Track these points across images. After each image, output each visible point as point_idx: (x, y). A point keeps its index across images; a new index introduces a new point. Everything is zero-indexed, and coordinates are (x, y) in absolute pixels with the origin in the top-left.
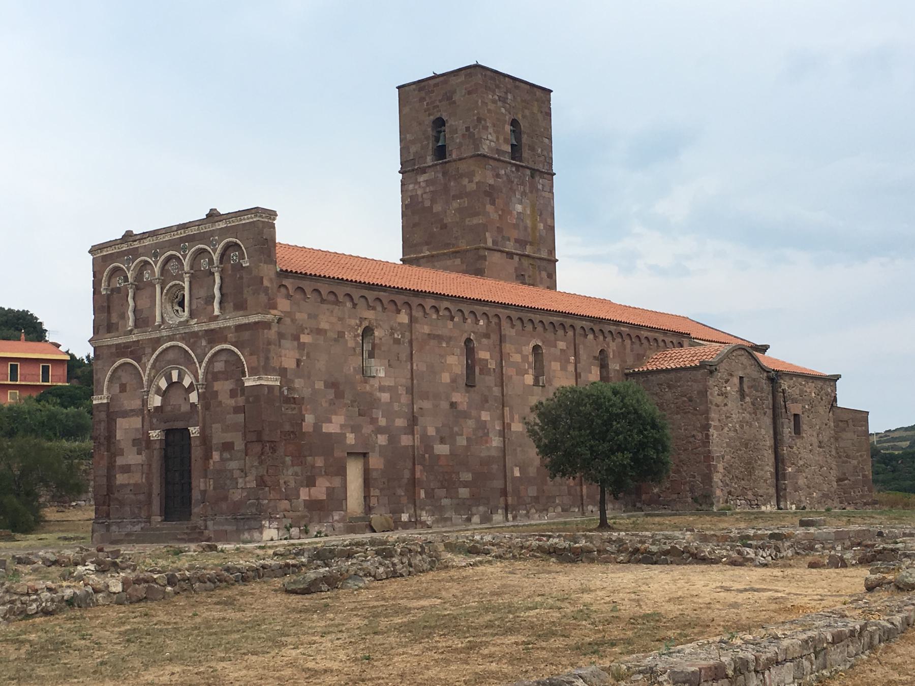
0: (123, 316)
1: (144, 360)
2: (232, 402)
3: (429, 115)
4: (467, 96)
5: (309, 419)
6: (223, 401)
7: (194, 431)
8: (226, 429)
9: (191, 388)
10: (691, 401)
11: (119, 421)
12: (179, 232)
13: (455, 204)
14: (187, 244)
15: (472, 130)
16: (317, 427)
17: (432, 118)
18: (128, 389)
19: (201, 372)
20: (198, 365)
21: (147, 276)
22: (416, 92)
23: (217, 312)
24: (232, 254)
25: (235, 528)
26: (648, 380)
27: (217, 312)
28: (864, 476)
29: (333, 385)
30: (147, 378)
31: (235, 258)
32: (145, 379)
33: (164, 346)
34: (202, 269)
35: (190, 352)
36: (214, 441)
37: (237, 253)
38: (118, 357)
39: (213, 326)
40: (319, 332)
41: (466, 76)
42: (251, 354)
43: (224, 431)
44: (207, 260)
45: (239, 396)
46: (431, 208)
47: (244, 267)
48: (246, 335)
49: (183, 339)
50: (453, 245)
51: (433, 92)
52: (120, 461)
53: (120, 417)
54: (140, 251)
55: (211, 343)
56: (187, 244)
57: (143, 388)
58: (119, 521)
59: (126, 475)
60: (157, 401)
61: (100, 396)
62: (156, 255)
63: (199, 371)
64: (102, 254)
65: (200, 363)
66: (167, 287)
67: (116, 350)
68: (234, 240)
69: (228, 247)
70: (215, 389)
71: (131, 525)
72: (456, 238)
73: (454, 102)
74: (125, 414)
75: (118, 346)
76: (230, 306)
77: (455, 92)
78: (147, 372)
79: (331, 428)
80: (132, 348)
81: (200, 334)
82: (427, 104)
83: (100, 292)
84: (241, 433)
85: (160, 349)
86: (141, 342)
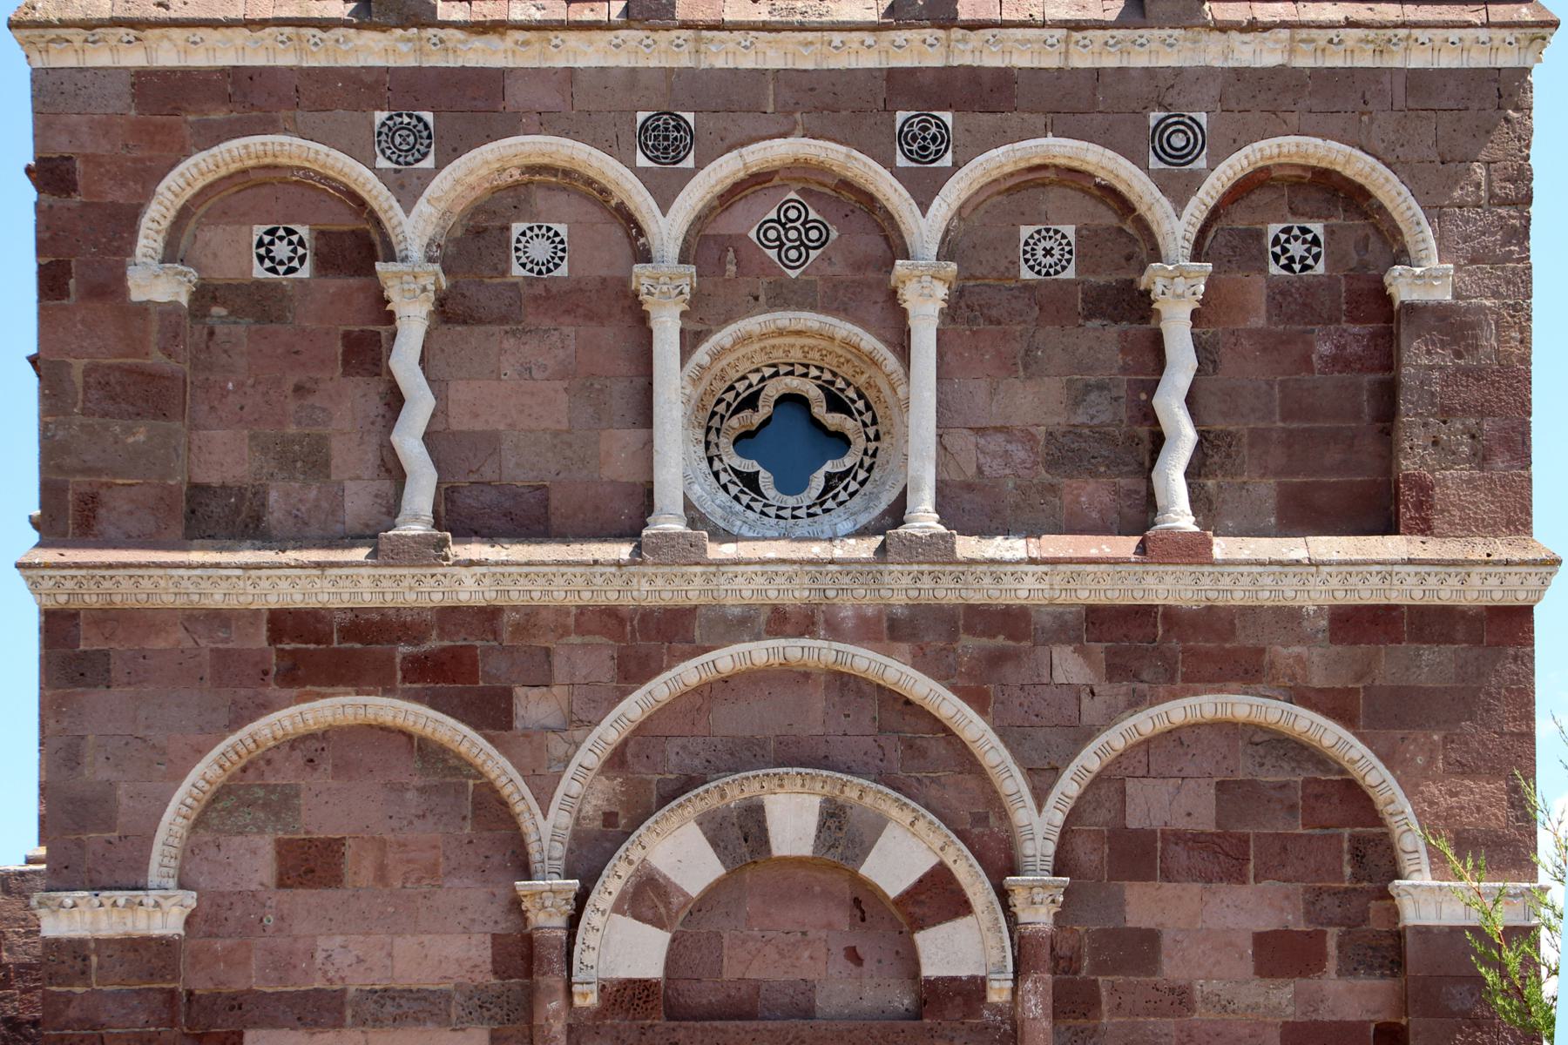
14: (947, 117)
31: (1296, 249)
44: (1070, 231)
54: (517, 97)
56: (947, 117)
66: (723, 337)
83: (110, 287)
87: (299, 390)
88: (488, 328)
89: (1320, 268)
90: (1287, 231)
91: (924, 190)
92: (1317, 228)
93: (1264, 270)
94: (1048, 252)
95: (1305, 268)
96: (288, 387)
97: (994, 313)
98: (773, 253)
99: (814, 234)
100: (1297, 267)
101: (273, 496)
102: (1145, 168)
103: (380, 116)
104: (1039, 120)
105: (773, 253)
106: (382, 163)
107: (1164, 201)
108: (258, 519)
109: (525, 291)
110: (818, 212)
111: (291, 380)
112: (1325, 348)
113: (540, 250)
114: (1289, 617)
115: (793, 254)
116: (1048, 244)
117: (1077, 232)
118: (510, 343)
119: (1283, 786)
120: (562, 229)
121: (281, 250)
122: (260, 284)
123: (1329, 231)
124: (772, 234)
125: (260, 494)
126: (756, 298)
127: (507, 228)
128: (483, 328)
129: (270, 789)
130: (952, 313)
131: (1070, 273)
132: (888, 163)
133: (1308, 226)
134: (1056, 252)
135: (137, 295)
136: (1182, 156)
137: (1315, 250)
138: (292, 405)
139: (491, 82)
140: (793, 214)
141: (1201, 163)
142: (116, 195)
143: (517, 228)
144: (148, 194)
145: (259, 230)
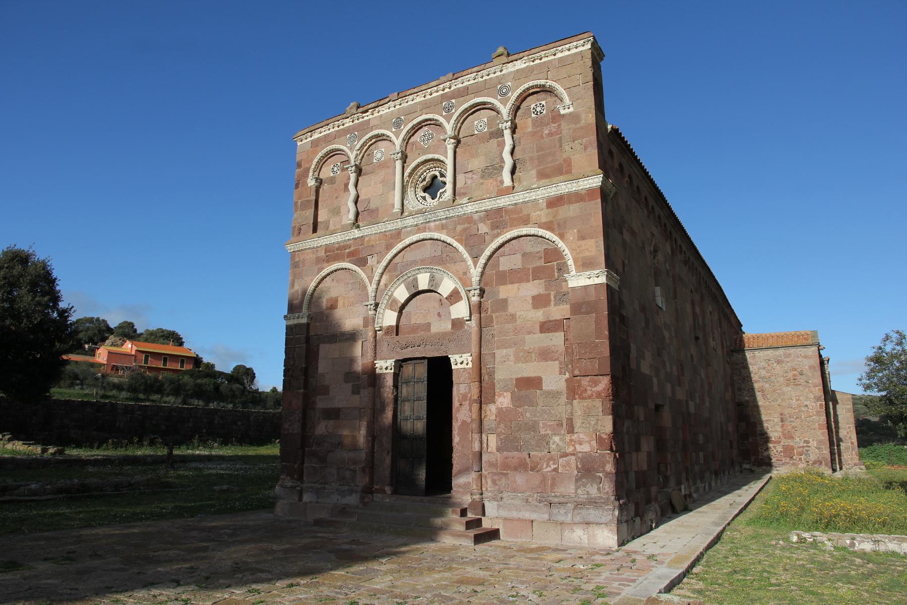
0: (336, 212)
1: (371, 262)
2: (539, 315)
5: (633, 347)
6: (518, 314)
8: (526, 356)
9: (454, 297)
10: (801, 374)
11: (325, 350)
12: (441, 86)
14: (453, 101)
16: (638, 364)
19: (475, 273)
20: (470, 262)
25: (546, 516)
26: (755, 356)
27: (507, 180)
28: (852, 443)
29: (643, 309)
30: (374, 286)
31: (539, 109)
32: (371, 289)
33: (407, 241)
34: (476, 132)
35: (456, 244)
36: (499, 376)
38: (328, 261)
39: (504, 201)
40: (633, 233)
42: (582, 237)
43: (517, 360)
44: (485, 120)
45: (552, 303)
47: (564, 115)
49: (443, 228)
52: (321, 403)
53: (324, 343)
55: (498, 227)
57: (368, 301)
58: (319, 486)
59: (332, 422)
60: (389, 318)
61: (297, 315)
62: (398, 124)
63: (472, 270)
64: (313, 138)
65: (475, 258)
67: (325, 253)
68: (542, 82)
69: (524, 97)
70: (502, 295)
71: (339, 495)
75: (328, 248)
76: (528, 175)
78: (376, 278)
79: (645, 368)
80: (352, 249)
81: (476, 217)
84: (557, 362)
85: (400, 246)
86: (366, 239)
87: (337, 197)
88: (369, 175)
90: (536, 105)
92: (543, 103)
93: (531, 116)
94: (481, 126)
95: (541, 113)
96: (335, 197)
97: (469, 144)
98: (422, 143)
99: (431, 136)
100: (539, 113)
101: (331, 222)
102: (497, 99)
103: (348, 136)
104: (473, 95)
105: (422, 143)
106: (348, 145)
107: (502, 105)
109: (376, 165)
110: (431, 131)
112: (546, 132)
113: (379, 155)
115: (426, 142)
116: (480, 124)
117: (488, 120)
118: (373, 177)
120: (383, 150)
121: (335, 169)
122: (332, 177)
123: (546, 102)
124: (422, 139)
125: (329, 221)
126: (419, 154)
127: (373, 153)
128: (368, 176)
131: (486, 130)
133: (541, 103)
134: (483, 126)
135: (309, 185)
136: (505, 94)
137: (543, 108)
140: (426, 133)
141: (510, 94)
142: (307, 166)
143: (375, 152)
144: (312, 163)
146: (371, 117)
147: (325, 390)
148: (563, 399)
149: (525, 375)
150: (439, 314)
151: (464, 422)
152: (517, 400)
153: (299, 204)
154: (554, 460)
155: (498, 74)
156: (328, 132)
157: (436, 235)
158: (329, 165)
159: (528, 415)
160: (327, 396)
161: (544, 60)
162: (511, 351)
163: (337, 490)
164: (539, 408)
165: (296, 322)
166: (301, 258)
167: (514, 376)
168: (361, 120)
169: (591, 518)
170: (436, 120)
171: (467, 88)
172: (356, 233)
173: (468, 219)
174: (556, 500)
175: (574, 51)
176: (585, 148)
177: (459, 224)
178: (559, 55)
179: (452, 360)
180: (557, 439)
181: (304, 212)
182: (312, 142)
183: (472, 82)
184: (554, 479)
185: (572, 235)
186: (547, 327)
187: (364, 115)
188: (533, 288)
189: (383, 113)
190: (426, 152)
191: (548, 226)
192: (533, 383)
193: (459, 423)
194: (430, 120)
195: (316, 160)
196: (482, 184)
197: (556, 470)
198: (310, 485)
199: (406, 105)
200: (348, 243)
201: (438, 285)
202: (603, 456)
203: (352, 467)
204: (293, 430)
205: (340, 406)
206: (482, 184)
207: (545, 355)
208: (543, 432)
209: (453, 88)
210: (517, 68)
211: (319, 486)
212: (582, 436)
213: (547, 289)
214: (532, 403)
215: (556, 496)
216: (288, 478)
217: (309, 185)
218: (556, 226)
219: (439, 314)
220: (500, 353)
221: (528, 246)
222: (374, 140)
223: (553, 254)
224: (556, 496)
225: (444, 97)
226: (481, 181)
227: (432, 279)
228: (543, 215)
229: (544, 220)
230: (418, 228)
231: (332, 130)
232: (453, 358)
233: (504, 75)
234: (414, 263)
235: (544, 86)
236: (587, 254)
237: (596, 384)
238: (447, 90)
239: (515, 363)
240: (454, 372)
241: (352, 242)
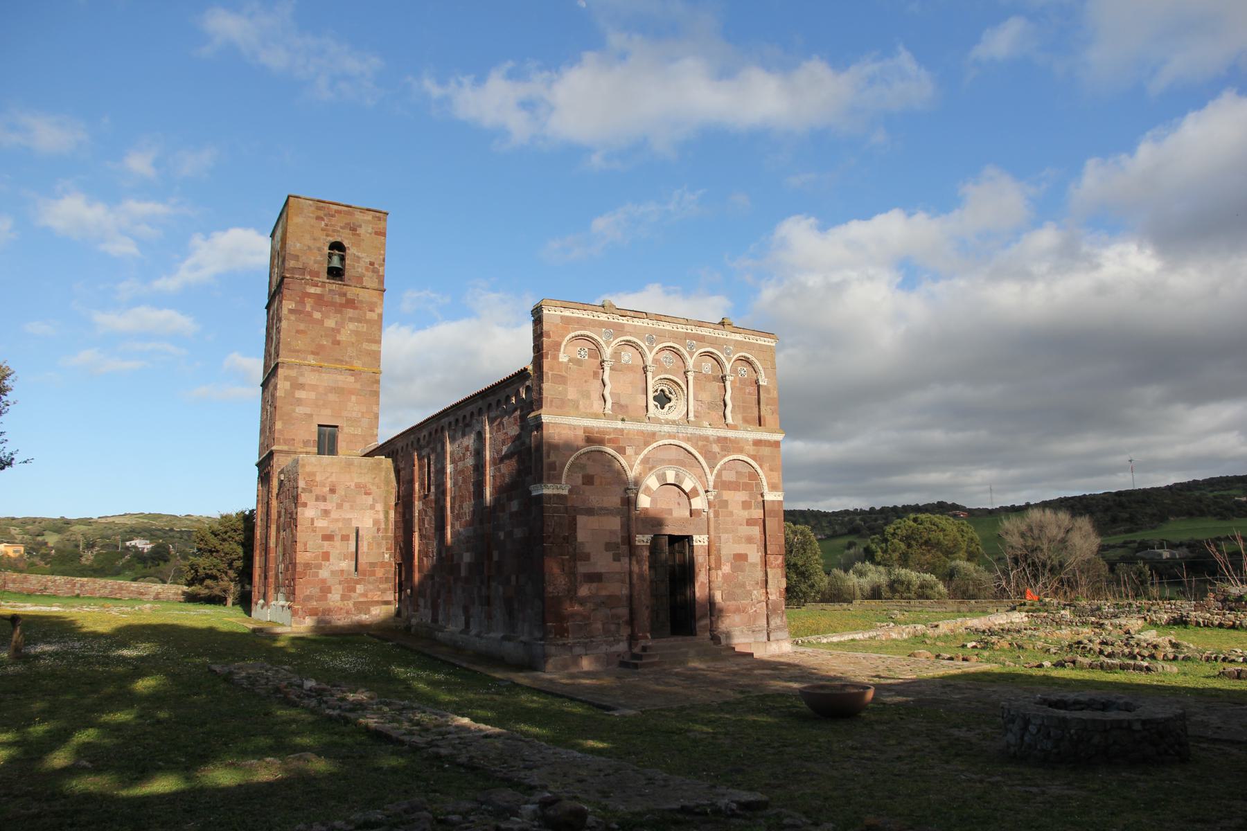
1: (629, 451)
2: (745, 514)
3: (327, 235)
4: (373, 235)
6: (734, 511)
7: (700, 541)
11: (581, 520)
13: (352, 326)
14: (694, 342)
15: (376, 266)
17: (332, 239)
18: (597, 481)
19: (711, 479)
20: (707, 470)
21: (626, 358)
22: (313, 209)
23: (730, 420)
24: (739, 368)
31: (743, 372)
33: (661, 443)
36: (723, 552)
37: (745, 369)
39: (731, 434)
41: (373, 217)
42: (771, 470)
45: (753, 507)
46: (321, 322)
48: (766, 451)
49: (688, 440)
50: (347, 363)
51: (333, 216)
53: (582, 514)
59: (595, 585)
63: (709, 476)
65: (712, 468)
70: (725, 498)
71: (607, 645)
72: (351, 357)
73: (359, 235)
74: (590, 512)
77: (360, 226)
80: (612, 436)
82: (326, 225)
86: (625, 431)
89: (746, 376)
91: (691, 355)
101: (581, 403)
103: (604, 330)
106: (604, 338)
108: (578, 407)
111: (585, 378)
112: (747, 391)
113: (626, 358)
114: (746, 440)
119: (746, 473)
121: (582, 353)
129: (581, 464)
130: (695, 378)
131: (710, 373)
132: (686, 350)
135: (560, 360)
136: (729, 354)
138: (584, 384)
139: (622, 325)
143: (623, 353)
145: (579, 348)
146: (626, 322)
147: (587, 557)
148: (759, 568)
149: (739, 552)
150: (679, 504)
151: (702, 582)
152: (735, 568)
153: (550, 375)
154: (755, 605)
155: (725, 336)
156: (581, 316)
157: (684, 445)
158: (576, 346)
159: (740, 578)
160: (587, 562)
161: (751, 341)
162: (731, 535)
163: (604, 641)
164: (746, 573)
165: (556, 492)
166: (557, 431)
167: (732, 553)
168: (616, 320)
169: (779, 637)
170: (679, 350)
171: (703, 336)
172: (620, 425)
173: (706, 439)
174: (757, 629)
175: (766, 343)
176: (772, 414)
177: (700, 440)
178: (759, 342)
179: (694, 539)
180: (755, 592)
181: (557, 386)
182: (562, 317)
183: (708, 334)
184: (755, 616)
185: (766, 466)
186: (750, 522)
187: (621, 318)
188: (741, 496)
189: (638, 324)
190: (666, 371)
191: (754, 458)
192: (741, 557)
193: (699, 583)
194: (674, 348)
195: (568, 338)
196: (709, 413)
197: (755, 611)
198: (577, 641)
199: (657, 326)
200: (608, 430)
201: (681, 482)
202: (781, 601)
203: (616, 621)
204: (558, 593)
205: (603, 570)
206: (709, 413)
207: (750, 540)
208: (748, 588)
209: (694, 331)
210: (736, 338)
211: (586, 640)
212: (772, 590)
213: (750, 498)
214: (743, 571)
215: (757, 627)
216: (558, 637)
217: (560, 360)
218: (758, 459)
219: (679, 504)
220: (724, 536)
221: (740, 465)
222: (624, 343)
223: (754, 476)
224: (757, 627)
225: (688, 336)
226: (707, 411)
227: (677, 475)
228: (751, 449)
229: (752, 453)
230: (671, 436)
231: (586, 316)
232: (695, 537)
233: (728, 339)
234: (662, 461)
235: (749, 358)
236: (774, 481)
237: (776, 559)
238: (689, 331)
239: (733, 543)
240: (695, 548)
241: (612, 430)
